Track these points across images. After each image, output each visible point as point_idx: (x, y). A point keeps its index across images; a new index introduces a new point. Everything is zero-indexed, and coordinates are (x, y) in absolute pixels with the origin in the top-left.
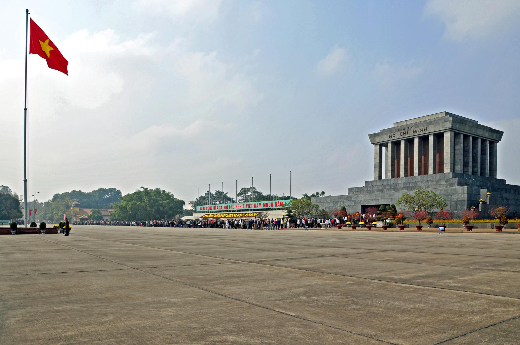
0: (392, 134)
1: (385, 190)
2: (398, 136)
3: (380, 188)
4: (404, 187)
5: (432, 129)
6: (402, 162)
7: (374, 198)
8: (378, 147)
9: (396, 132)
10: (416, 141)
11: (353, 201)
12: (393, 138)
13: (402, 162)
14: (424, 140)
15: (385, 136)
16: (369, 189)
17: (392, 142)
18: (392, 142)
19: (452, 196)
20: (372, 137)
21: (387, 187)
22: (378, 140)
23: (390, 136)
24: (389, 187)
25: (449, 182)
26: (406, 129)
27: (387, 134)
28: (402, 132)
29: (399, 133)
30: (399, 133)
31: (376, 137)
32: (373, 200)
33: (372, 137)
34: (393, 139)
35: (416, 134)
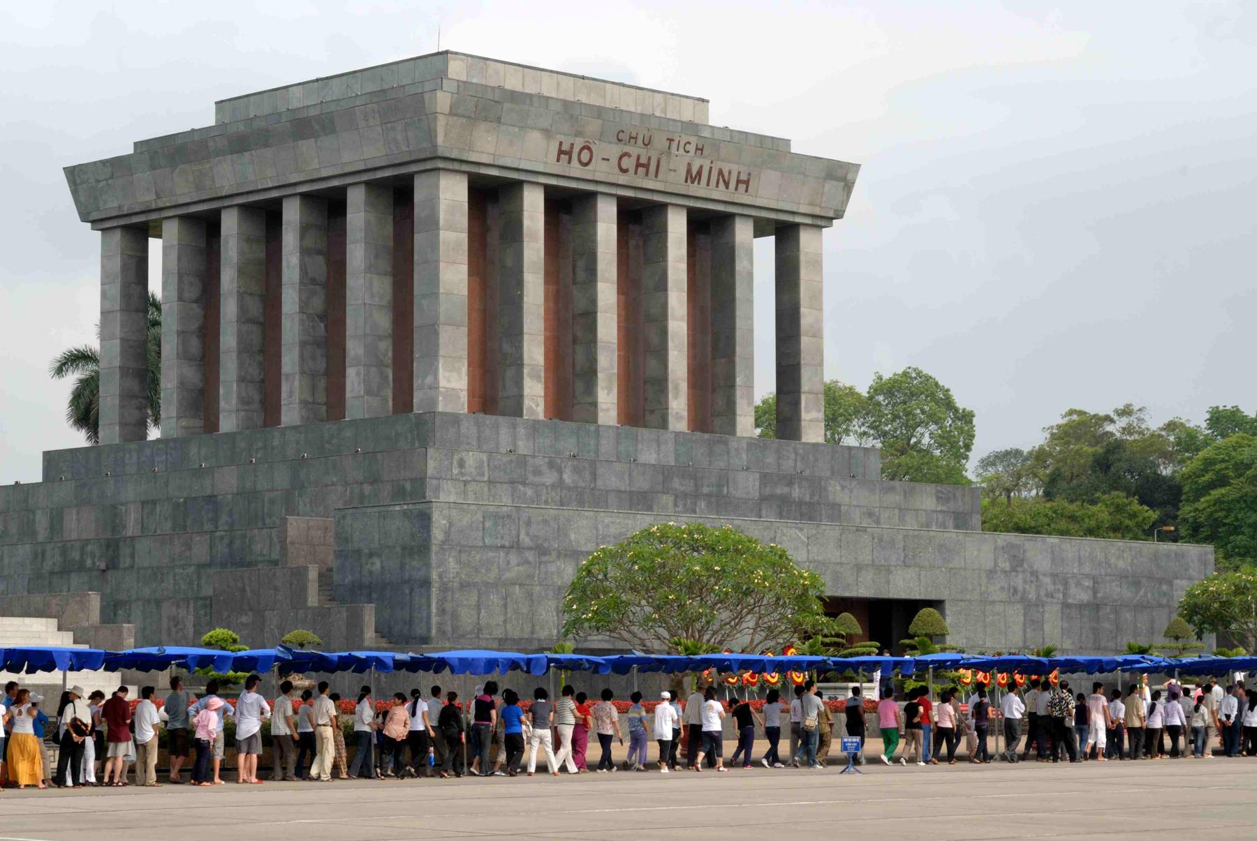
1: (667, 499)
3: (642, 483)
4: (763, 499)
5: (769, 193)
6: (608, 328)
7: (865, 557)
9: (602, 136)
12: (576, 170)
15: (535, 137)
16: (568, 477)
17: (548, 190)
18: (548, 190)
19: (1170, 583)
21: (676, 484)
23: (564, 153)
24: (689, 486)
25: (952, 506)
26: (660, 142)
27: (547, 133)
28: (634, 150)
29: (614, 151)
30: (614, 151)
31: (483, 126)
32: (859, 568)
34: (574, 174)
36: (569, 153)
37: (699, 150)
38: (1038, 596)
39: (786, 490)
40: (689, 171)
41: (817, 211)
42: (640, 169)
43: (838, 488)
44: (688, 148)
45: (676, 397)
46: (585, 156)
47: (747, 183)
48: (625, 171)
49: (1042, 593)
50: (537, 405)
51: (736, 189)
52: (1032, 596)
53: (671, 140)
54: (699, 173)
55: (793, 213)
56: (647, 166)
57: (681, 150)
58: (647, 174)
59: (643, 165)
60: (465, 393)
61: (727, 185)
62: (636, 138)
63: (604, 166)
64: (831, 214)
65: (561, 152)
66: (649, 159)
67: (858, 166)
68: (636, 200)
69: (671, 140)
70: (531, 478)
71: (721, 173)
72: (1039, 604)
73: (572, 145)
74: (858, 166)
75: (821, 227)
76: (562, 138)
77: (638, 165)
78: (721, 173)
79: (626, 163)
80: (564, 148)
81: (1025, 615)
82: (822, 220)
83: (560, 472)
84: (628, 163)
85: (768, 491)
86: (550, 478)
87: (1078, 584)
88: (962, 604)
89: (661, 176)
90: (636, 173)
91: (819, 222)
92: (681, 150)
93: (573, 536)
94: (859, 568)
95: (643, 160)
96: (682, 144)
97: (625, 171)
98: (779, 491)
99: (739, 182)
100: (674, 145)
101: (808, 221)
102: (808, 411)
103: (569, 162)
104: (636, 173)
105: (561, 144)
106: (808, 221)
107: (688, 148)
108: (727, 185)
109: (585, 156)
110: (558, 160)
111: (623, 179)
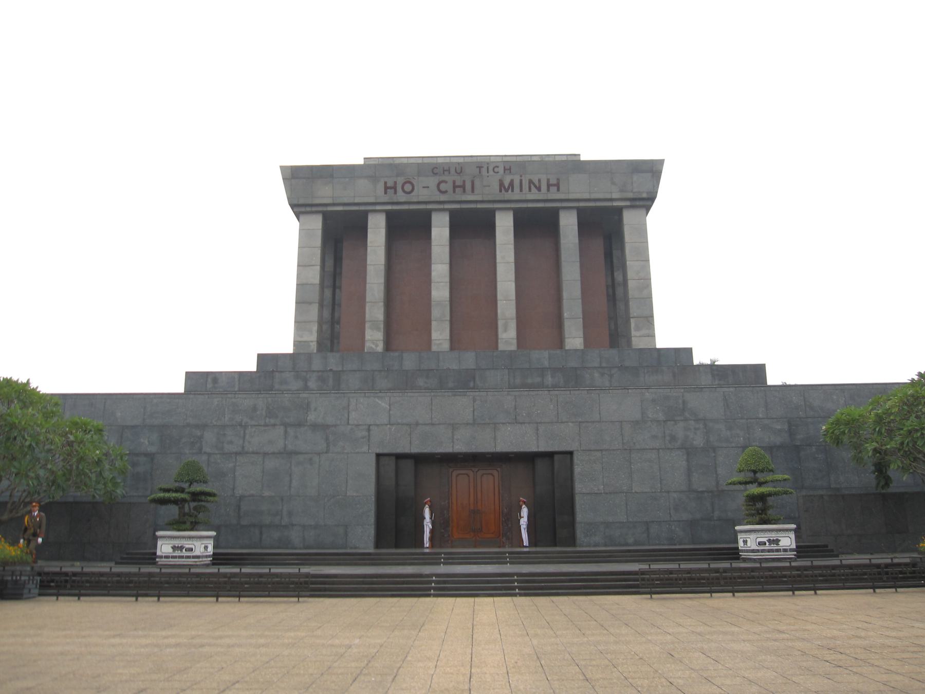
0: (400, 181)
2: (425, 191)
6: (440, 292)
8: (316, 223)
10: (504, 224)
11: (315, 427)
13: (440, 292)
22: (325, 193)
29: (432, 182)
30: (432, 182)
32: (454, 427)
35: (509, 196)
36: (394, 188)
39: (538, 380)
40: (501, 184)
41: (630, 195)
42: (457, 190)
43: (596, 375)
44: (496, 170)
45: (505, 330)
46: (408, 187)
47: (558, 186)
48: (446, 192)
50: (377, 346)
51: (548, 190)
52: (699, 441)
53: (480, 168)
54: (512, 184)
55: (611, 200)
56: (463, 187)
57: (491, 172)
58: (464, 191)
59: (459, 187)
60: (315, 343)
61: (539, 189)
62: (449, 171)
63: (425, 191)
64: (645, 195)
65: (386, 188)
66: (464, 181)
67: (661, 162)
68: (461, 210)
69: (480, 168)
70: (277, 386)
71: (531, 182)
73: (395, 183)
74: (661, 162)
75: (648, 208)
76: (386, 179)
77: (455, 187)
78: (531, 182)
79: (443, 187)
80: (388, 185)
81: (688, 461)
82: (646, 201)
83: (306, 380)
84: (448, 187)
85: (518, 381)
86: (296, 385)
88: (599, 454)
89: (476, 192)
90: (454, 192)
91: (638, 203)
92: (491, 172)
93: (119, 414)
94: (454, 427)
95: (458, 183)
96: (491, 168)
97: (446, 192)
98: (529, 381)
99: (549, 186)
100: (484, 170)
101: (628, 203)
102: (638, 329)
103: (395, 192)
104: (454, 192)
105: (386, 183)
106: (628, 203)
107: (496, 170)
108: (539, 189)
109: (408, 187)
110: (386, 193)
111: (443, 198)
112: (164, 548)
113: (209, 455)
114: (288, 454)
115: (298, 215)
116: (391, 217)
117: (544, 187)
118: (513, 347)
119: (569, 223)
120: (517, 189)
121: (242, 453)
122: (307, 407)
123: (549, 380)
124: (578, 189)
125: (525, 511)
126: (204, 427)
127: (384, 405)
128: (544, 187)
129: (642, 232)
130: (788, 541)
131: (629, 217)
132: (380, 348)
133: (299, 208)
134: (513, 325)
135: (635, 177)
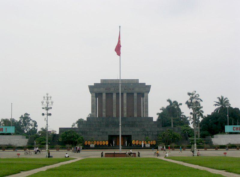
2: (112, 91)
8: (94, 95)
11: (101, 132)
14: (130, 95)
20: (91, 88)
30: (113, 88)
33: (91, 88)
37: (125, 87)
38: (148, 134)
46: (109, 89)
47: (134, 89)
49: (148, 134)
52: (146, 134)
61: (131, 90)
63: (112, 90)
67: (151, 86)
72: (148, 135)
74: (151, 86)
75: (148, 93)
77: (117, 89)
78: (129, 89)
82: (148, 92)
87: (155, 132)
99: (132, 89)
112: (91, 146)
113: (88, 135)
114: (98, 135)
115: (91, 93)
116: (106, 93)
117: (131, 90)
118: (126, 116)
119: (135, 95)
120: (127, 90)
121: (92, 135)
122: (99, 129)
123: (131, 123)
124: (137, 90)
125: (126, 142)
126: (87, 132)
127: (109, 129)
128: (131, 90)
129: (147, 97)
130: (149, 146)
131: (145, 94)
132: (105, 116)
133: (91, 92)
134: (126, 112)
135: (147, 88)
